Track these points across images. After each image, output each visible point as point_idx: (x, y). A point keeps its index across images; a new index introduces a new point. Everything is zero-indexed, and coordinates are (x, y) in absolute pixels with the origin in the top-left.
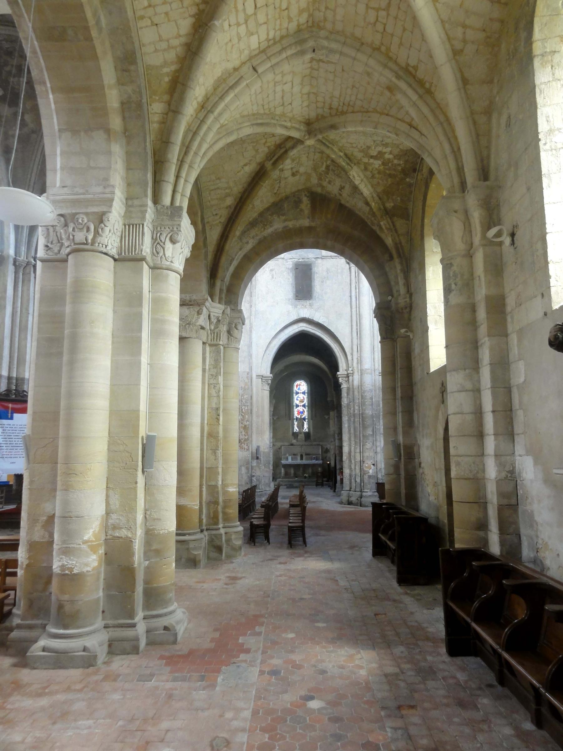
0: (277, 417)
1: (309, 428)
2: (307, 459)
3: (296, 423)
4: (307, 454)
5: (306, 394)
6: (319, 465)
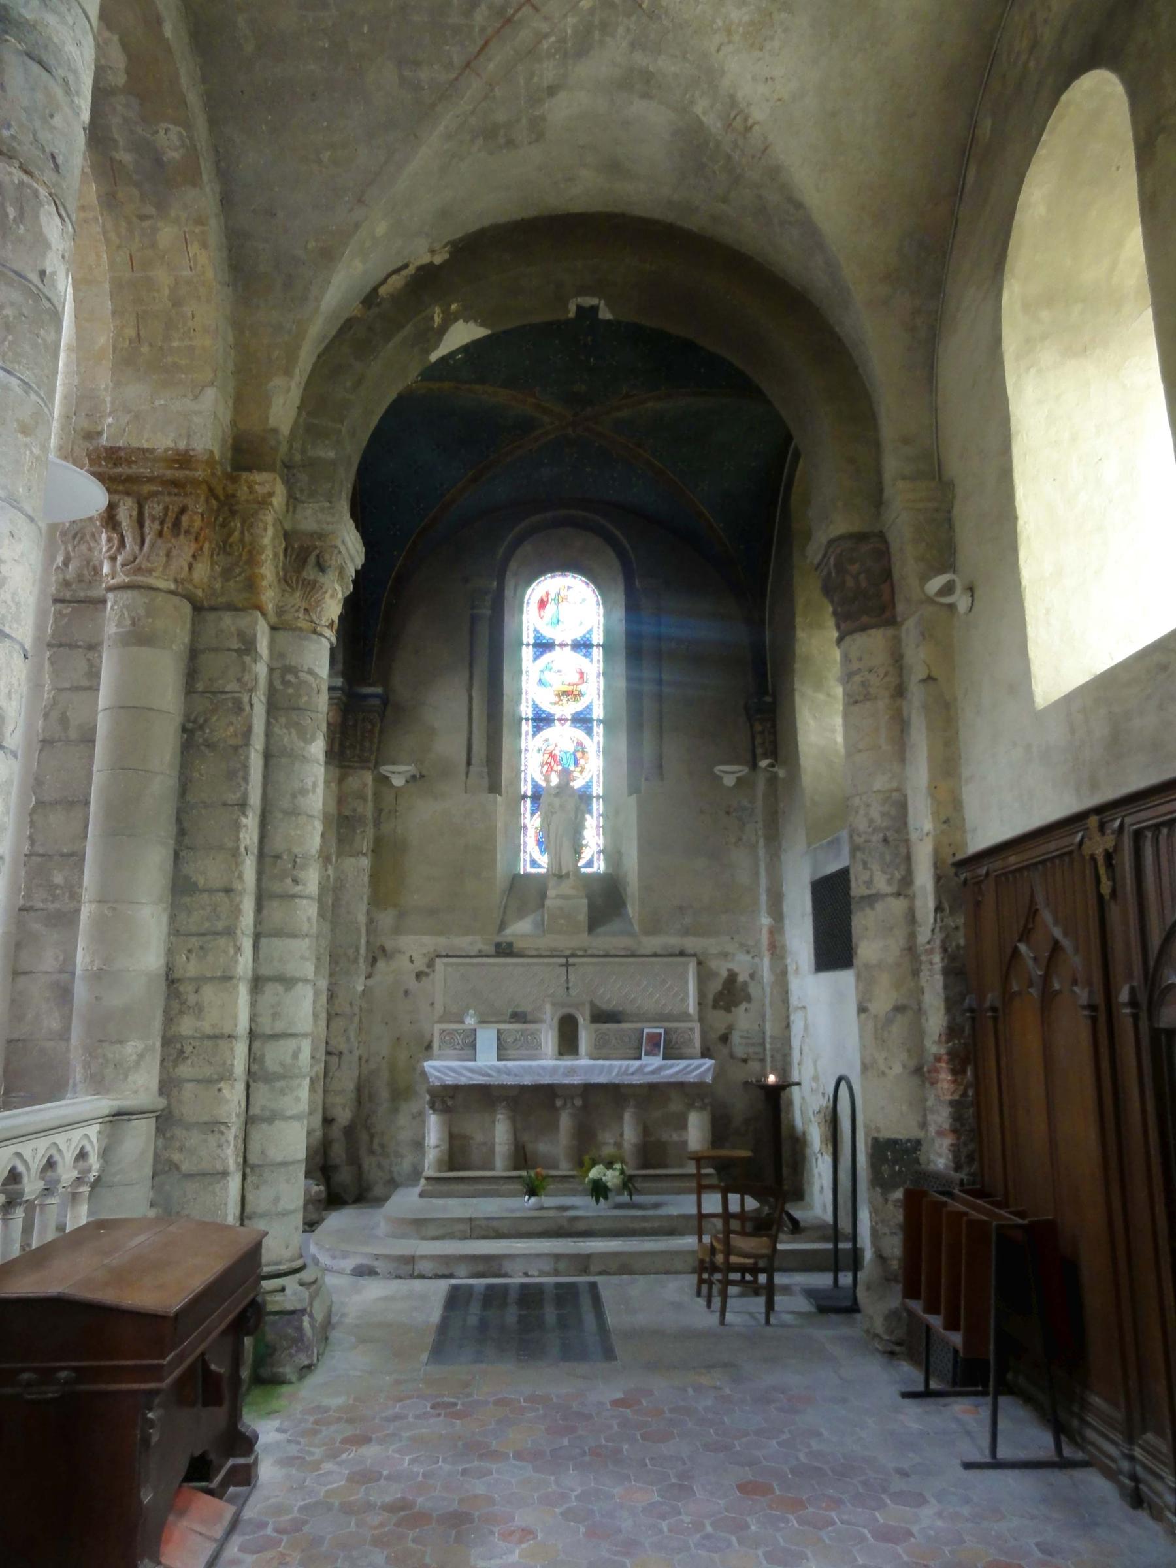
0: (407, 769)
1: (612, 854)
2: (601, 1050)
3: (532, 822)
4: (601, 1017)
5: (598, 654)
6: (692, 1093)
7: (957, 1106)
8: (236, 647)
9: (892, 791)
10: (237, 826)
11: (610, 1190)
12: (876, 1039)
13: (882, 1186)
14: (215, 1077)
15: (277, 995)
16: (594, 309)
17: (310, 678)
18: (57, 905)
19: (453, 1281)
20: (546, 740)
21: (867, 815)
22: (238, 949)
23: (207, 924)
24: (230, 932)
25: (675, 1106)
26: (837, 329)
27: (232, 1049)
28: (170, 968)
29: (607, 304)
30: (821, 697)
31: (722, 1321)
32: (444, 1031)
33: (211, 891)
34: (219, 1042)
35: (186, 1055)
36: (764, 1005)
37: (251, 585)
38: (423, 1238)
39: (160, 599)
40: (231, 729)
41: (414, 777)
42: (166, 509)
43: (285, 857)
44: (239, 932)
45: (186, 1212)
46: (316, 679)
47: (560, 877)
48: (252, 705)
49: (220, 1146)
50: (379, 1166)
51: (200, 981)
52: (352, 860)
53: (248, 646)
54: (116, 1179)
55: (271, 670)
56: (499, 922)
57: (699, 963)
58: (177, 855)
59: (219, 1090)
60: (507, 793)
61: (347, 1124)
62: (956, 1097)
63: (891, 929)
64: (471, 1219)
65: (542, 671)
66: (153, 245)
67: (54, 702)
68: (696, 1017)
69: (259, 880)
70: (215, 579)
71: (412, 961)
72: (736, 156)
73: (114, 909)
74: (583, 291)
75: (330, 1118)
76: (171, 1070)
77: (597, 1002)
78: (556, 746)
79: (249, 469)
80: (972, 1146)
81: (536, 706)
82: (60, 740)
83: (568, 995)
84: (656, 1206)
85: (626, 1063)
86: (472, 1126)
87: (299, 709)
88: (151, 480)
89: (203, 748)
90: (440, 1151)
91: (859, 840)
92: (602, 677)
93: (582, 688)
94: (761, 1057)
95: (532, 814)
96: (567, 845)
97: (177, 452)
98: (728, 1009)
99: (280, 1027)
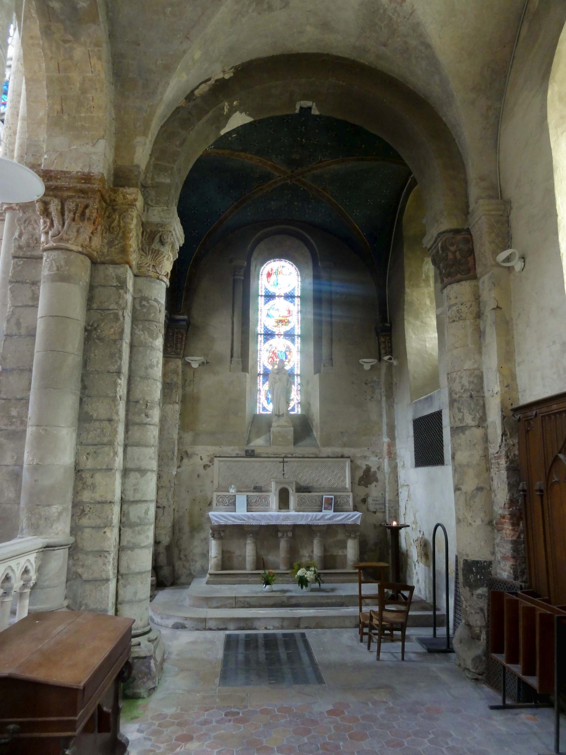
0: (201, 359)
1: (306, 404)
2: (301, 507)
4: (300, 489)
5: (297, 301)
7: (515, 543)
8: (115, 284)
9: (474, 369)
10: (115, 384)
11: (308, 582)
12: (466, 505)
13: (470, 586)
14: (102, 525)
15: (137, 479)
16: (310, 108)
17: (155, 304)
18: (13, 427)
19: (227, 632)
20: (271, 345)
21: (460, 382)
22: (116, 453)
23: (98, 439)
24: (111, 443)
25: (341, 536)
26: (444, 119)
27: (112, 509)
28: (77, 464)
29: (316, 105)
30: (418, 323)
31: (378, 659)
32: (219, 496)
33: (101, 420)
34: (104, 505)
35: (86, 513)
36: (384, 484)
37: (124, 250)
38: (210, 608)
39: (73, 256)
40: (112, 330)
41: (203, 363)
42: (77, 205)
43: (141, 402)
44: (116, 443)
45: (85, 602)
46: (158, 305)
47: (279, 416)
48: (124, 317)
49: (104, 564)
50: (184, 567)
51: (94, 471)
52: (171, 406)
53: (122, 285)
54: (46, 583)
55: (134, 299)
56: (247, 439)
57: (351, 461)
58: (81, 400)
59: (105, 532)
60: (251, 372)
61: (167, 545)
62: (514, 538)
63: (475, 445)
64: (235, 598)
65: (269, 310)
66: (71, 58)
67: (13, 313)
68: (350, 490)
69: (127, 415)
70: (104, 246)
71: (201, 459)
72: (394, 18)
73: (46, 430)
74: (306, 97)
75: (158, 541)
76: (77, 521)
77: (298, 481)
78: (276, 348)
79: (123, 186)
80: (523, 566)
81: (265, 328)
82: (16, 335)
83: (284, 478)
84: (333, 590)
85: (315, 513)
86: (234, 546)
87: (150, 321)
88: (68, 189)
89: (96, 340)
90: (218, 560)
91: (456, 397)
92: (299, 313)
93: (290, 319)
94: (384, 511)
95: (263, 383)
96: (283, 400)
97: (83, 174)
98: (367, 487)
99: (138, 497)
